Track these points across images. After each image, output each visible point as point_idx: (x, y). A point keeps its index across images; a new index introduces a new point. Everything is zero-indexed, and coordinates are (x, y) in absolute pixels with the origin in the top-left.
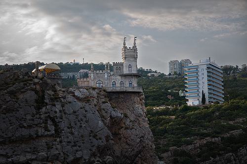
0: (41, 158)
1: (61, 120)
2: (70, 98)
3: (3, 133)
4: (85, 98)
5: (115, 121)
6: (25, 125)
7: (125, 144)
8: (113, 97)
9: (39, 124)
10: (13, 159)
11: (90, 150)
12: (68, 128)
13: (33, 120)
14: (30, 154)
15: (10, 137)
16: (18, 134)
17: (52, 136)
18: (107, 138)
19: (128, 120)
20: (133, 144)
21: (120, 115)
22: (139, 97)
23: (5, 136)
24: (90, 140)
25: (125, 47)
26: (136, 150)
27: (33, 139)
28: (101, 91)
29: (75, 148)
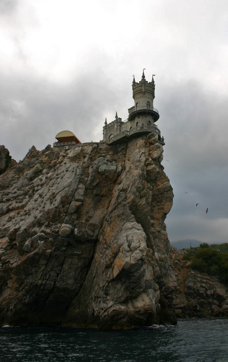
8: (120, 149)
25: (134, 82)
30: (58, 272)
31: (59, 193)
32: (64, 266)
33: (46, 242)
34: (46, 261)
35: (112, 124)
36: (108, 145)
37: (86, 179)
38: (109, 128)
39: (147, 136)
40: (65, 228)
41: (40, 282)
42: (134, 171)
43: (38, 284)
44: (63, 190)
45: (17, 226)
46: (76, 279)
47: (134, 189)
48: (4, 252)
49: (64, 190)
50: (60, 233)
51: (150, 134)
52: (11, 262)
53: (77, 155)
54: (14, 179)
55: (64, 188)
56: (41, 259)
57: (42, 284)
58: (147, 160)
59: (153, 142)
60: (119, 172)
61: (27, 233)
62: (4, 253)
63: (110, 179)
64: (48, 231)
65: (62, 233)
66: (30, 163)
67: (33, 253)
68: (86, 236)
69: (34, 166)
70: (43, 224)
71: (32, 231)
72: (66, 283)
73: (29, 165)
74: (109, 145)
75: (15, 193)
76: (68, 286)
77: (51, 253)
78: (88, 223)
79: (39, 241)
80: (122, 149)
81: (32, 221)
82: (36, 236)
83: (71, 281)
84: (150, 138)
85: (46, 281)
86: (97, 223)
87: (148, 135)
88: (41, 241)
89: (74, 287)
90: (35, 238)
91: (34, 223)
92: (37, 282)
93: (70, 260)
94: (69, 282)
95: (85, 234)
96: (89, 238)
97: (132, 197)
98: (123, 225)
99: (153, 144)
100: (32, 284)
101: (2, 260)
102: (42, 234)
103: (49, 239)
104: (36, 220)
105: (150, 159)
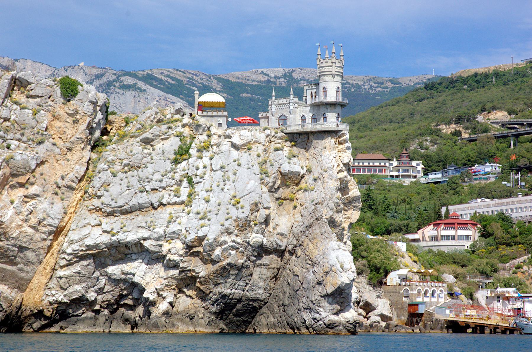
0: (155, 236)
1: (201, 180)
3: (112, 200)
4: (245, 145)
6: (148, 188)
9: (168, 186)
10: (118, 237)
11: (222, 225)
12: (207, 191)
13: (161, 181)
14: (144, 230)
15: (121, 207)
16: (134, 202)
17: (182, 203)
18: (256, 207)
21: (296, 168)
23: (114, 205)
24: (228, 209)
27: (155, 208)
28: (276, 133)
29: (202, 222)
30: (247, 281)
32: (254, 275)
33: (237, 251)
34: (237, 271)
37: (267, 179)
41: (229, 291)
42: (328, 181)
45: (200, 234)
47: (332, 205)
48: (182, 258)
50: (251, 243)
51: (342, 133)
54: (145, 155)
57: (230, 294)
58: (339, 165)
60: (303, 174)
61: (217, 243)
62: (181, 260)
64: (239, 240)
68: (275, 246)
70: (231, 233)
75: (161, 181)
76: (258, 296)
77: (243, 264)
78: (276, 232)
79: (230, 251)
81: (220, 229)
83: (260, 291)
86: (285, 233)
88: (232, 250)
89: (263, 297)
90: (226, 248)
92: (225, 291)
94: (258, 292)
95: (274, 243)
96: (278, 248)
97: (331, 213)
98: (328, 244)
99: (342, 144)
100: (220, 293)
101: (181, 268)
102: (234, 244)
103: (239, 249)
104: (224, 228)
105: (342, 165)
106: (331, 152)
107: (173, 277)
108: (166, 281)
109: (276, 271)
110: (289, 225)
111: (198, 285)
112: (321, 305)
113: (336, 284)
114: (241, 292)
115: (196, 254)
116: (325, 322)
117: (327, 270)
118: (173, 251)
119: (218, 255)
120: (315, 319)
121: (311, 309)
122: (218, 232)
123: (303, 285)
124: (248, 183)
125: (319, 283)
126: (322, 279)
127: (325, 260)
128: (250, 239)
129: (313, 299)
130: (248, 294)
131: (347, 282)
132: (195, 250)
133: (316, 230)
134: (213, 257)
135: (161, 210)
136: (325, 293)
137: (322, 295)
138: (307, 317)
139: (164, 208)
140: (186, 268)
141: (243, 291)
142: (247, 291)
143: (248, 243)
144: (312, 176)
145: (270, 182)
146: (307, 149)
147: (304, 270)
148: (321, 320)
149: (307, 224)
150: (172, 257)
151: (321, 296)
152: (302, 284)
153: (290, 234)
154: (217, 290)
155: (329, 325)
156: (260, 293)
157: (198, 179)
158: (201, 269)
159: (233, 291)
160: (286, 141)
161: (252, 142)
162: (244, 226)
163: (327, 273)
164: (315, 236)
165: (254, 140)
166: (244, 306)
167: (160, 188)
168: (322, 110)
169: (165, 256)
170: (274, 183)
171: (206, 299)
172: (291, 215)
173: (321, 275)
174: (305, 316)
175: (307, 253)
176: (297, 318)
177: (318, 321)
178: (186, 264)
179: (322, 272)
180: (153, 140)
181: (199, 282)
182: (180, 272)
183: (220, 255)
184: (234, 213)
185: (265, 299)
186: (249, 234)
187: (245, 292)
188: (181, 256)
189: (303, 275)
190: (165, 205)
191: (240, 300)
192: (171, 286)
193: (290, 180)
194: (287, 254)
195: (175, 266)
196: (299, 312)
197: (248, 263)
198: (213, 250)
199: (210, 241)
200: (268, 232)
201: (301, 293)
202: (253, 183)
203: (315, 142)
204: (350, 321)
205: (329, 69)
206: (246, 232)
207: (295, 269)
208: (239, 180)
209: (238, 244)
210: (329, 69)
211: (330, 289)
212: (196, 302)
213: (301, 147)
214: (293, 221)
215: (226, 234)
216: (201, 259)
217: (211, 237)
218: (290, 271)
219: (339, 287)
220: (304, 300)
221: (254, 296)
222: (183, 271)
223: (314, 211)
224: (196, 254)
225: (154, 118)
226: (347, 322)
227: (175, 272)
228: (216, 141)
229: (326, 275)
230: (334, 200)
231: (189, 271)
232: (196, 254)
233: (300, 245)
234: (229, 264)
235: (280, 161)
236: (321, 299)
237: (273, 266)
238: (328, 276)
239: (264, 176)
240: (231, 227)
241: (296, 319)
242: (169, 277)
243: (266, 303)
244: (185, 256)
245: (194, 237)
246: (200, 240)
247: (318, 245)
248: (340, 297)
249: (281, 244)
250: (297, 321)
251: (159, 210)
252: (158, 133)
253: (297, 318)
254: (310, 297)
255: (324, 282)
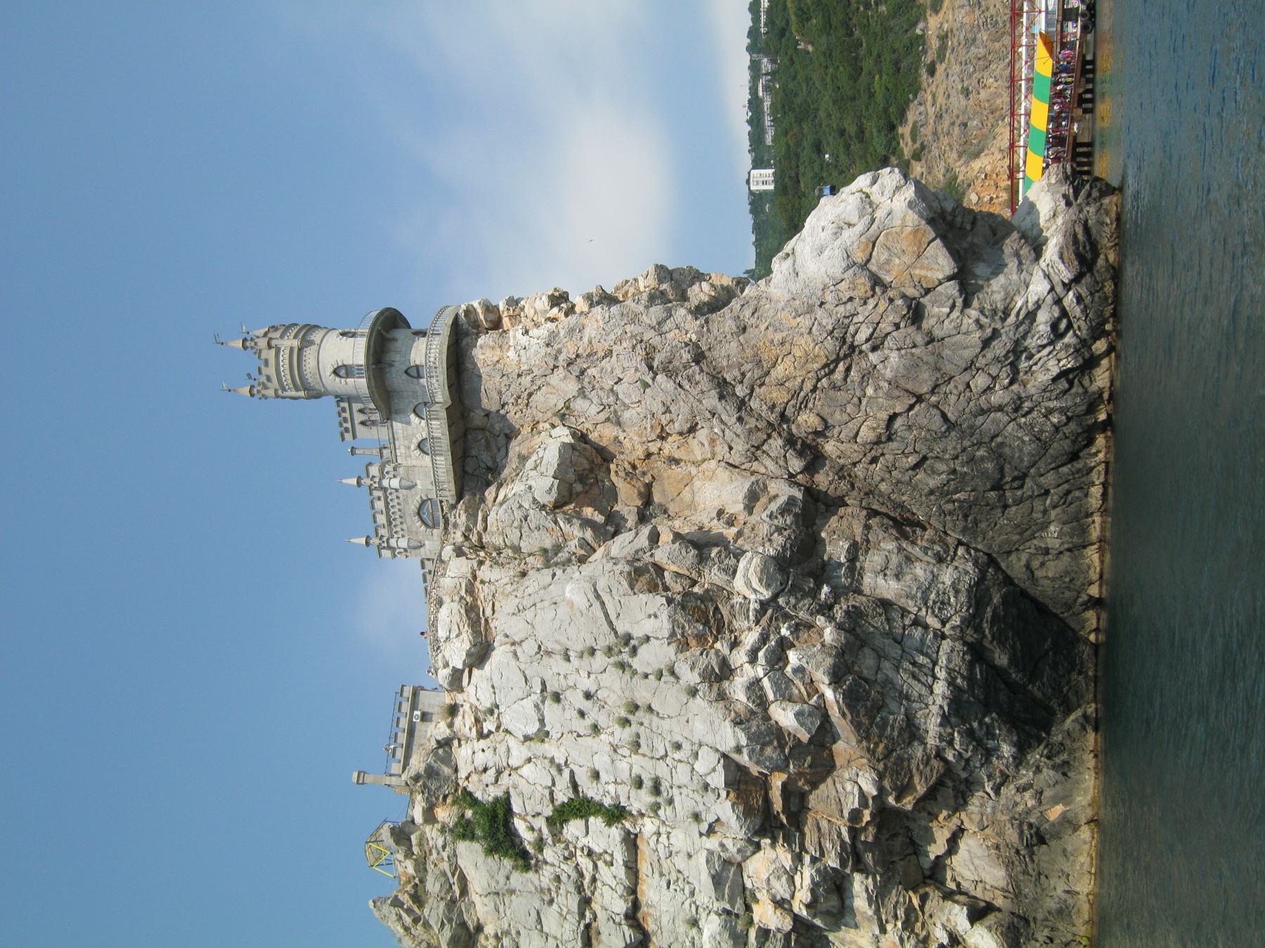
1: (566, 773)
2: (477, 691)
5: (581, 479)
7: (693, 442)
8: (485, 457)
9: (580, 888)
11: (693, 692)
18: (645, 575)
19: (579, 405)
20: (685, 409)
22: (478, 335)
26: (711, 400)
28: (455, 525)
30: (907, 622)
31: (610, 623)
32: (888, 595)
34: (867, 651)
35: (380, 505)
36: (458, 502)
37: (573, 545)
38: (390, 523)
39: (467, 334)
40: (751, 570)
41: (940, 688)
42: (586, 340)
43: (948, 693)
44: (603, 604)
46: (940, 560)
48: (807, 859)
49: (606, 598)
50: (766, 594)
52: (856, 805)
53: (469, 618)
55: (598, 597)
56: (856, 668)
57: (951, 683)
59: (492, 317)
60: (574, 435)
61: (755, 720)
62: (814, 860)
63: (591, 470)
65: (768, 586)
66: (442, 895)
67: (829, 694)
69: (463, 880)
70: (724, 663)
71: (744, 699)
72: (952, 594)
73: (453, 901)
74: (460, 497)
76: (963, 587)
77: (840, 627)
79: (789, 669)
80: (488, 447)
81: (705, 704)
82: (766, 683)
83: (947, 576)
84: (476, 324)
85: (937, 669)
86: (747, 485)
87: (465, 326)
88: (787, 662)
89: (970, 566)
90: (776, 685)
91: (714, 695)
92: (939, 701)
93: (868, 580)
94: (948, 583)
95: (779, 522)
99: (500, 319)
100: (945, 720)
101: (843, 863)
102: (761, 654)
106: (511, 343)
107: (877, 899)
108: (889, 927)
109: (874, 522)
110: (723, 474)
111: (908, 803)
112: (1000, 306)
113: (916, 232)
114: (946, 645)
115: (794, 801)
116: (1066, 274)
117: (863, 283)
118: (781, 889)
119: (798, 715)
120: (1054, 326)
121: (1017, 350)
122: (716, 712)
123: (924, 389)
124: (571, 604)
125: (916, 314)
126: (900, 302)
127: (829, 297)
128: (752, 597)
129: (976, 337)
130: (956, 621)
131: (909, 192)
132: (778, 805)
133: (727, 353)
134: (804, 737)
135: (650, 921)
136: (952, 288)
137: (959, 302)
138: (1047, 366)
139: (644, 909)
140: (843, 843)
141: (944, 637)
142: (944, 623)
143: (764, 605)
144: (579, 405)
145: (580, 535)
146: (510, 434)
147: (870, 391)
148: (1058, 302)
149: (714, 393)
150: (803, 895)
151: (967, 304)
152: (920, 399)
153: (752, 473)
154: (931, 733)
155: (1080, 258)
156: (955, 575)
157: (563, 782)
158: (849, 786)
159: (941, 674)
160: (483, 500)
161: (469, 599)
162: (702, 615)
163: (876, 281)
164: (749, 352)
165: (463, 593)
166: (999, 639)
167: (582, 916)
168: (397, 379)
169: (796, 918)
170: (587, 523)
171: (964, 775)
172: (694, 470)
173: (883, 305)
174: (1043, 378)
175: (808, 386)
176: (1050, 412)
177: (1064, 313)
178: (828, 845)
179: (871, 303)
180: (463, 925)
181: (898, 799)
182: (860, 871)
183: (797, 707)
184: (655, 655)
185: (976, 564)
186: (737, 600)
187: (947, 630)
188: (798, 859)
189: (889, 396)
190: (636, 905)
191: (976, 652)
192: (910, 910)
193: (587, 475)
194: (823, 480)
195: (833, 889)
196: (1027, 405)
197: (839, 613)
198: (778, 733)
199: (744, 741)
200: (740, 541)
201: (953, 399)
202: (571, 588)
203: (485, 403)
204: (1064, 196)
205: (284, 356)
206: (725, 611)
207: (866, 434)
208: (563, 640)
209: (764, 639)
210: (284, 356)
211: (939, 263)
212: (977, 818)
213: (503, 451)
214: (713, 463)
215: (726, 684)
216: (814, 785)
217: (729, 737)
218: (874, 460)
219: (931, 222)
220: (981, 381)
221: (963, 598)
222: (853, 855)
223: (670, 373)
224: (797, 802)
225: (409, 911)
226: (1068, 204)
227: (860, 886)
228: (470, 720)
229: (885, 287)
230: (641, 308)
231: (854, 832)
232: (794, 801)
233: (783, 417)
234: (836, 681)
235: (527, 506)
236: (975, 303)
237: (858, 530)
238: (887, 278)
239: (563, 556)
240: (702, 662)
241: (1055, 419)
242: (877, 912)
243: (992, 561)
244: (803, 848)
245: (728, 804)
246: (741, 783)
247: (778, 337)
248: (970, 236)
249: (782, 500)
250: (1062, 411)
251: (650, 926)
252: (442, 904)
253: (1050, 412)
254: (968, 354)
255: (911, 292)
